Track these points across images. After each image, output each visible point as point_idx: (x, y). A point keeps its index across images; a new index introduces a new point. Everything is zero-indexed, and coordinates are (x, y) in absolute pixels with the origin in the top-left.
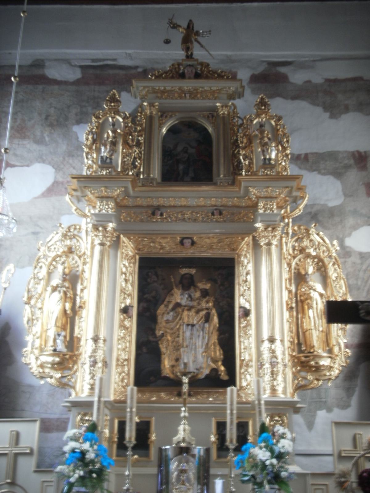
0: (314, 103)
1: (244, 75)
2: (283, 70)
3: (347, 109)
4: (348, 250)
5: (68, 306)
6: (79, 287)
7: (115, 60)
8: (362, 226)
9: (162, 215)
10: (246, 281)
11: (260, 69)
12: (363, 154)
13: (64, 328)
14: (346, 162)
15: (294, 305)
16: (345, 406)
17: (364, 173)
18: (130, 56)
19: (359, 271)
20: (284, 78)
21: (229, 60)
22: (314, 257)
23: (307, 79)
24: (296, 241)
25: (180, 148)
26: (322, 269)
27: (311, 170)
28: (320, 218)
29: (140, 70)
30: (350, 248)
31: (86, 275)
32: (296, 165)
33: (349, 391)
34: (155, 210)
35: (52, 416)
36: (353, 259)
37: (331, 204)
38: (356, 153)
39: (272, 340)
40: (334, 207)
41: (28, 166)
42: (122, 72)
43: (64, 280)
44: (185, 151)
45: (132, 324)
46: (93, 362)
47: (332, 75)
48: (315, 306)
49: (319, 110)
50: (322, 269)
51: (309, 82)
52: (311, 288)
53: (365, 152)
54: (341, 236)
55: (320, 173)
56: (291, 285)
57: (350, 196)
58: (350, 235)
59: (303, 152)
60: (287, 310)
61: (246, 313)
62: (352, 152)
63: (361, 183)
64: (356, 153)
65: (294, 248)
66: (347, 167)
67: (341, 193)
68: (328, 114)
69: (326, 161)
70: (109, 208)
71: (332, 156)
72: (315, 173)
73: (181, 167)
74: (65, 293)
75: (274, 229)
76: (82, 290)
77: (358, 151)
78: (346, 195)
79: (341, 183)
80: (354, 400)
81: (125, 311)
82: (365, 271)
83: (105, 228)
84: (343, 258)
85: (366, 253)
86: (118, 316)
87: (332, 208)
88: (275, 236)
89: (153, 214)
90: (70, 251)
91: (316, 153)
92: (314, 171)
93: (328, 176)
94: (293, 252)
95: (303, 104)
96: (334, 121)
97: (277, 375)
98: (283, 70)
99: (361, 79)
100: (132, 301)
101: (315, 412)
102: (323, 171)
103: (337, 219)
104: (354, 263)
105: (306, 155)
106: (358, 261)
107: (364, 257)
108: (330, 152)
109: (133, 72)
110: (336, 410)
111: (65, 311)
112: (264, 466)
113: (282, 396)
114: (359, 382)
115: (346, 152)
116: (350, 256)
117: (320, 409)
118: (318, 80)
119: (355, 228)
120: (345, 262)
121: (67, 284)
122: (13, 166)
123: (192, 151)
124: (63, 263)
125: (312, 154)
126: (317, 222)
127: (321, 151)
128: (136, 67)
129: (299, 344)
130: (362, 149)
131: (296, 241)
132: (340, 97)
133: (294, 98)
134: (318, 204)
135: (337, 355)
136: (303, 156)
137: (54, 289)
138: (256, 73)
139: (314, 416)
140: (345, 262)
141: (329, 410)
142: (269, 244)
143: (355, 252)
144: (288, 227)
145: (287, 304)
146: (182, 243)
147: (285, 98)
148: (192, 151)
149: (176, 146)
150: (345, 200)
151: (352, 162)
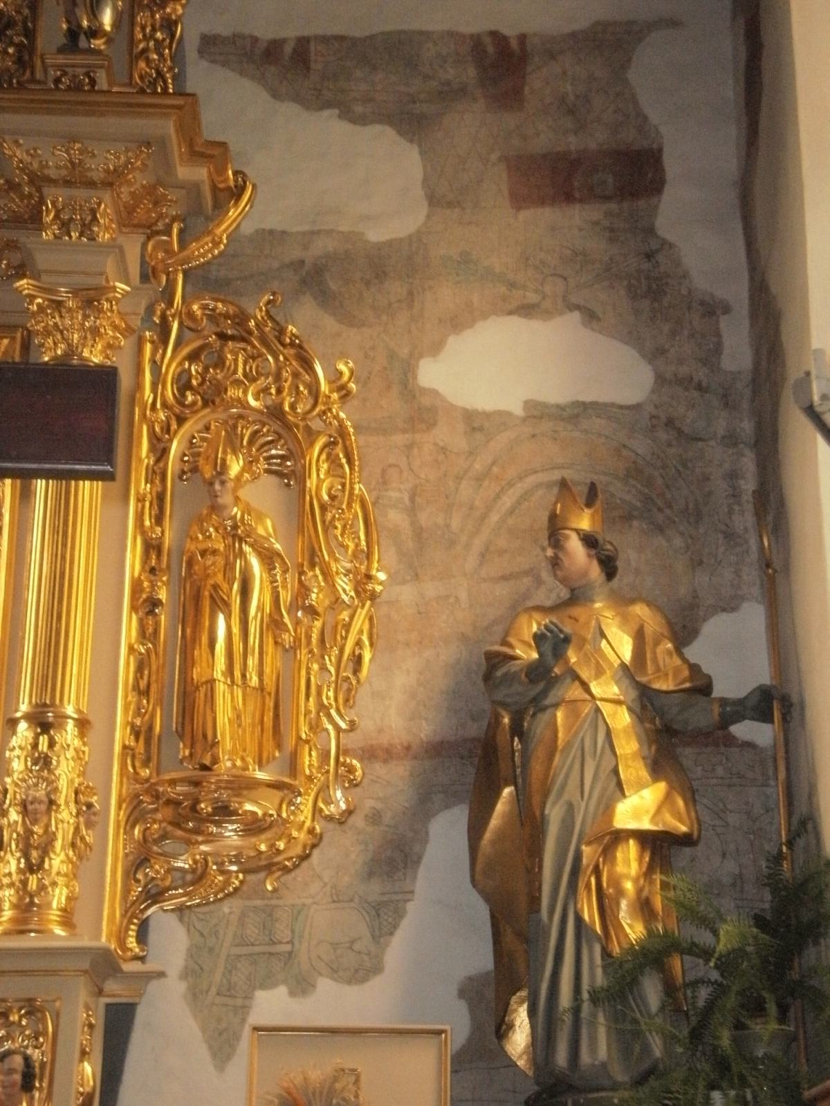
4: (426, 401)
8: (485, 316)
12: (514, 44)
14: (450, 73)
17: (511, 120)
19: (459, 479)
24: (193, 357)
27: (316, 101)
30: (434, 393)
32: (261, 80)
36: (446, 434)
37: (375, 235)
38: (487, 40)
39: (43, 722)
40: (389, 243)
52: (236, 535)
53: (523, 38)
54: (404, 352)
55: (347, 114)
56: (159, 520)
57: (450, 205)
58: (436, 348)
59: (291, 33)
60: (134, 608)
62: (472, 36)
63: (494, 157)
64: (487, 40)
65: (184, 385)
66: (450, 94)
67: (419, 192)
69: (374, 68)
77: (494, 34)
78: (433, 200)
79: (422, 153)
82: (480, 479)
84: (404, 431)
85: (488, 415)
87: (379, 246)
88: (95, 332)
91: (341, 38)
92: (328, 105)
93: (377, 129)
94: (180, 401)
97: (46, 848)
101: (249, 997)
102: (359, 109)
103: (396, 289)
104: (443, 450)
105: (303, 44)
106: (459, 442)
107: (481, 429)
108: (390, 33)
110: (325, 985)
113: (59, 931)
115: (451, 34)
116: (432, 425)
117: (268, 982)
119: (457, 323)
120: (410, 447)
125: (325, 40)
126: (326, 299)
127: (358, 33)
131: (193, 357)
134: (329, 232)
135: (310, 779)
136: (288, 49)
140: (410, 447)
143: (453, 407)
144: (170, 303)
145: (137, 587)
150: (428, 217)
151: (472, 72)
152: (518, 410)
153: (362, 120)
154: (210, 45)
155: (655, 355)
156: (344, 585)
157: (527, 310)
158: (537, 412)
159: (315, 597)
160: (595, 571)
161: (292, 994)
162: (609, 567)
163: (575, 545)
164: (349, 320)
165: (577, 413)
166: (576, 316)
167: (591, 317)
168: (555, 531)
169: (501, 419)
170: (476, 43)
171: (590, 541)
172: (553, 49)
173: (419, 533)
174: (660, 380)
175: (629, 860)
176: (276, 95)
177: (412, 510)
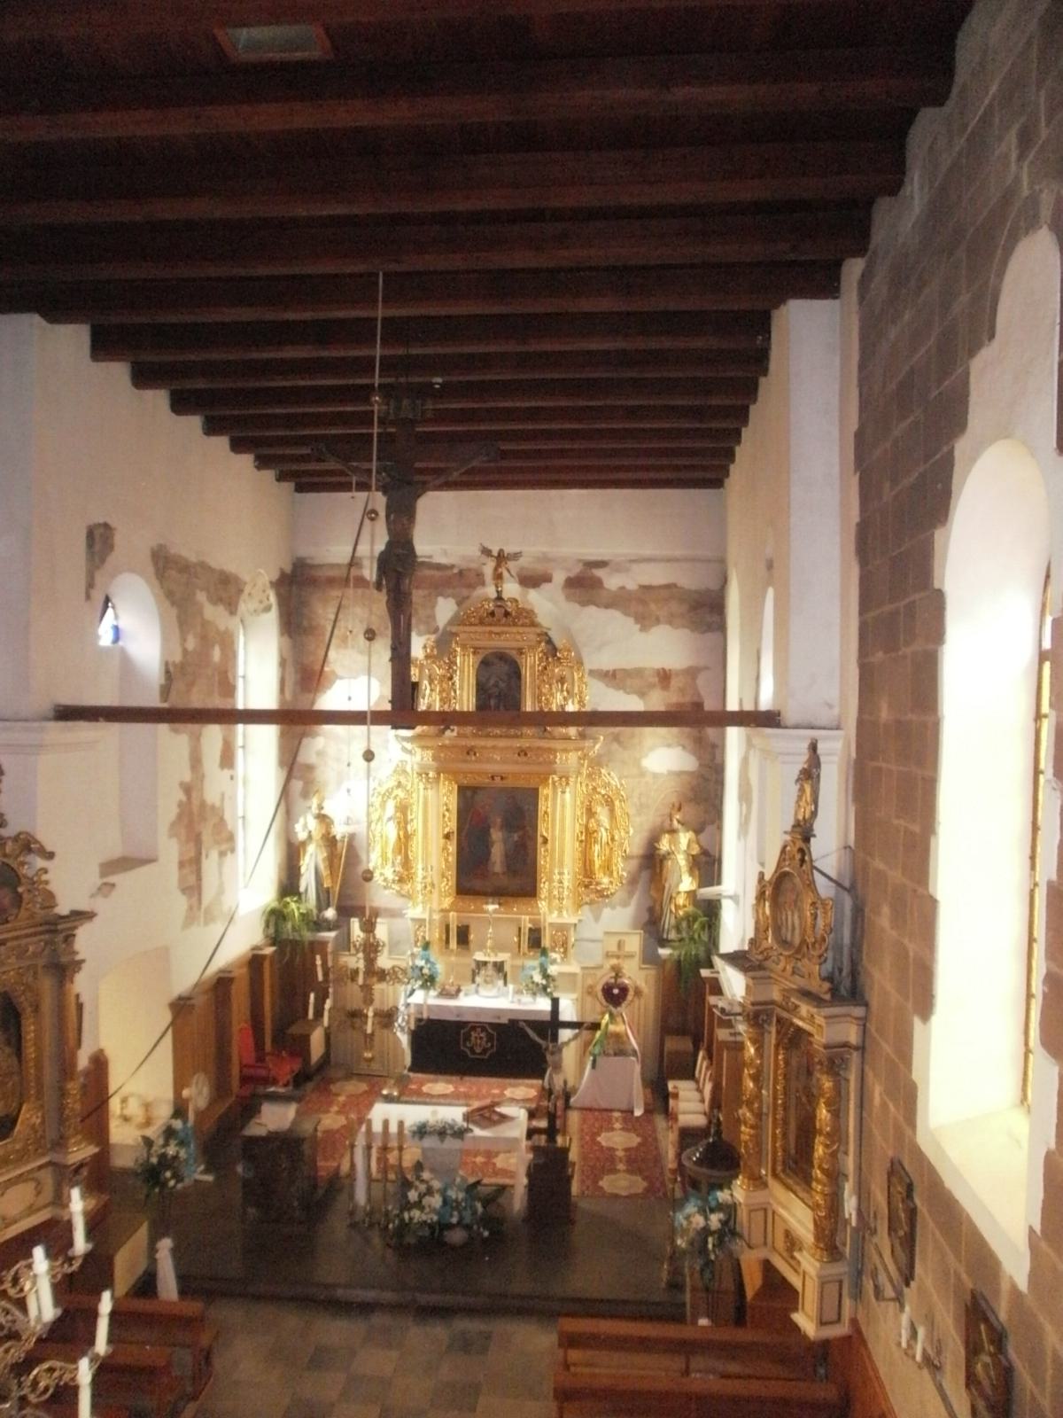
0: (626, 614)
1: (559, 577)
2: (599, 573)
3: (658, 621)
5: (401, 833)
6: (409, 817)
7: (430, 557)
9: (475, 754)
10: (546, 812)
11: (576, 570)
13: (400, 853)
15: (583, 838)
16: (625, 904)
17: (666, 693)
18: (445, 553)
20: (597, 584)
21: (545, 558)
22: (603, 796)
23: (621, 584)
25: (492, 682)
26: (609, 803)
27: (618, 687)
28: (622, 739)
29: (456, 571)
31: (415, 807)
33: (631, 893)
34: (470, 751)
41: (355, 678)
42: (437, 574)
43: (396, 812)
44: (496, 685)
45: (452, 848)
47: (646, 580)
49: (631, 621)
50: (609, 803)
51: (623, 588)
58: (647, 755)
59: (611, 668)
61: (545, 841)
66: (652, 686)
68: (638, 626)
71: (638, 673)
72: (621, 692)
73: (492, 702)
74: (399, 823)
75: (567, 779)
76: (412, 820)
77: (663, 669)
80: (634, 901)
81: (447, 836)
83: (427, 774)
86: (442, 841)
89: (468, 753)
90: (399, 785)
92: (620, 689)
95: (615, 614)
96: (643, 635)
98: (599, 573)
99: (674, 585)
100: (452, 825)
105: (614, 671)
109: (449, 573)
111: (400, 838)
112: (537, 984)
114: (640, 887)
118: (631, 585)
119: (652, 749)
121: (398, 814)
122: (341, 678)
123: (502, 685)
124: (395, 798)
128: (452, 567)
129: (586, 870)
130: (667, 667)
132: (653, 606)
133: (607, 606)
137: (390, 819)
138: (572, 575)
139: (601, 912)
141: (613, 908)
142: (563, 792)
146: (493, 778)
147: (597, 606)
148: (502, 685)
149: (488, 680)
151: (657, 679)
152: (665, 772)
153: (628, 693)
154: (592, 673)
155: (699, 758)
156: (623, 833)
157: (669, 746)
158: (670, 773)
159: (616, 837)
160: (680, 826)
162: (683, 824)
163: (675, 822)
164: (625, 748)
165: (680, 774)
166: (680, 748)
167: (684, 747)
168: (671, 820)
169: (662, 774)
170: (658, 670)
171: (679, 822)
172: (678, 673)
173: (641, 805)
174: (700, 765)
175: (681, 900)
176: (607, 685)
177: (639, 798)
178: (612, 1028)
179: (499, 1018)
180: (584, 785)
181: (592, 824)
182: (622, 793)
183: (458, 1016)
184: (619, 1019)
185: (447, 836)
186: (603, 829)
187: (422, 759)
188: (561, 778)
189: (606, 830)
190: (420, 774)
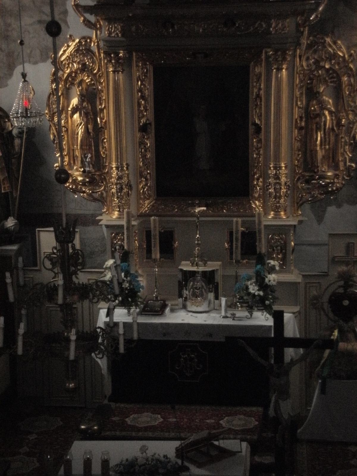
9: (173, 27)
10: (258, 96)
15: (303, 124)
22: (327, 70)
35: (87, 212)
46: (119, 189)
48: (323, 127)
70: (116, 30)
75: (284, 53)
76: (102, 110)
81: (144, 129)
83: (117, 54)
90: (84, 68)
100: (149, 115)
112: (254, 295)
139: (324, 211)
141: (339, 206)
142: (279, 69)
161: (337, 207)
178: (342, 345)
179: (211, 335)
180: (304, 59)
181: (314, 107)
182: (351, 66)
183: (164, 335)
184: (351, 336)
185: (144, 129)
186: (327, 113)
187: (110, 33)
188: (276, 51)
189: (331, 112)
190: (107, 54)
